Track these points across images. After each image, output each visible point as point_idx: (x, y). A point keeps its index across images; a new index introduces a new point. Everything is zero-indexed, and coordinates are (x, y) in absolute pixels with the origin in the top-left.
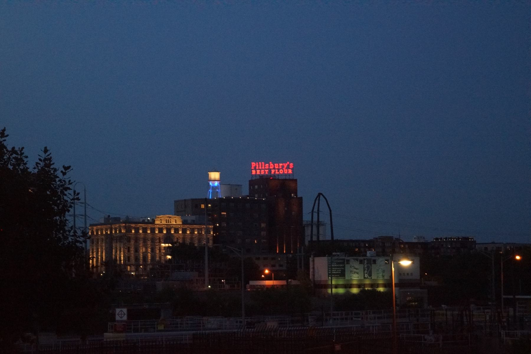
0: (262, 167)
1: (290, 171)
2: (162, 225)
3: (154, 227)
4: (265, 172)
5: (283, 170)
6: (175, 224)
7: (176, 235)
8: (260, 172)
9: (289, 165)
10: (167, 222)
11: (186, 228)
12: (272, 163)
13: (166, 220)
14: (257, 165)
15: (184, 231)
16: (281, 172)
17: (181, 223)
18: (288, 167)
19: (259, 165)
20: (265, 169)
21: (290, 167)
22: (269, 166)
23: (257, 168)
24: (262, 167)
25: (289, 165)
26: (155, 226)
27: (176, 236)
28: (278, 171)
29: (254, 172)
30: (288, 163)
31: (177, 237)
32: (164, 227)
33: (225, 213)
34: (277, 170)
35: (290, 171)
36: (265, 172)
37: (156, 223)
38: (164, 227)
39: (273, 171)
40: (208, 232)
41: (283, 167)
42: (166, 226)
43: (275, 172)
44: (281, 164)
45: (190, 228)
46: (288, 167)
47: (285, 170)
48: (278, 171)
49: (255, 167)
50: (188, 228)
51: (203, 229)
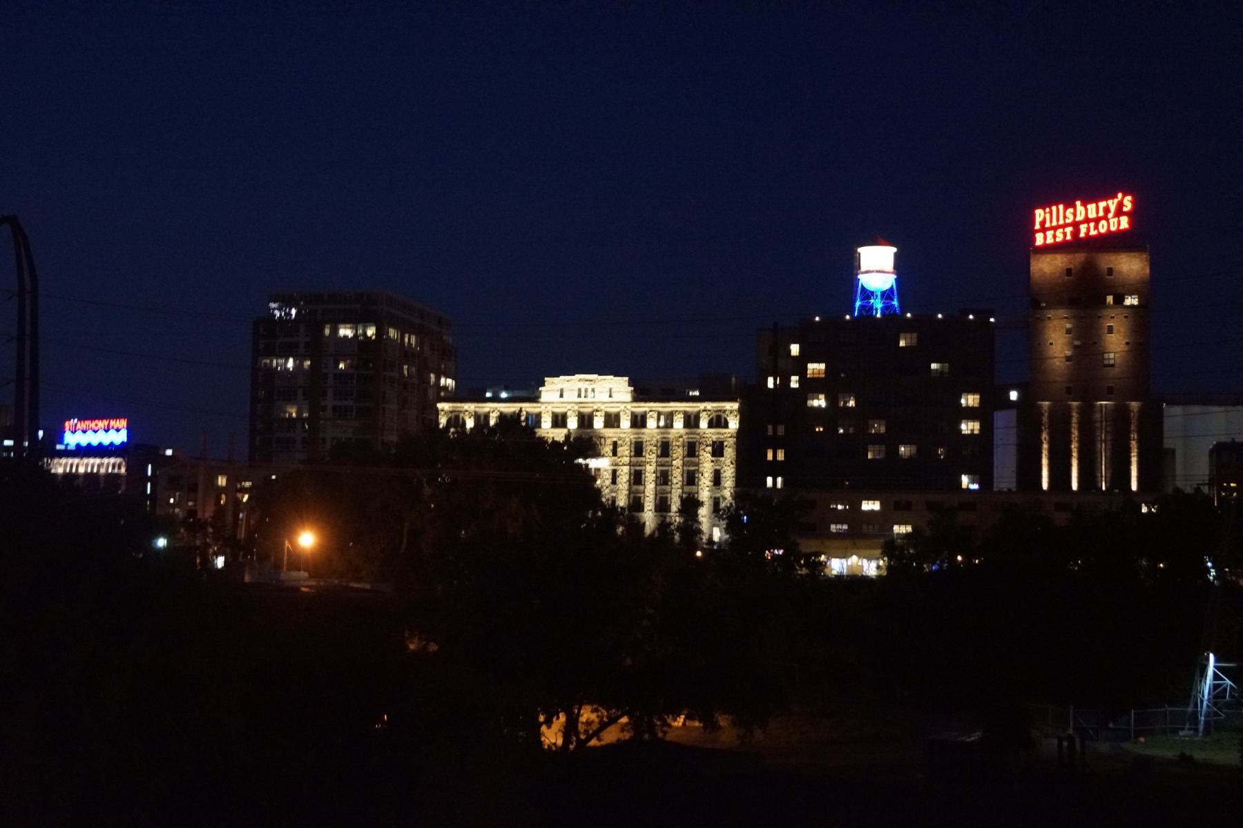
0: (1058, 220)
1: (1124, 223)
2: (564, 405)
3: (537, 410)
4: (1065, 234)
5: (1107, 220)
6: (610, 400)
7: (609, 432)
8: (1055, 237)
9: (1121, 205)
10: (583, 394)
11: (645, 412)
12: (1082, 205)
13: (580, 390)
14: (1048, 216)
15: (639, 421)
16: (1103, 229)
17: (629, 397)
18: (1119, 212)
19: (1051, 213)
20: (1065, 225)
21: (1125, 209)
22: (1075, 215)
23: (1048, 225)
24: (1058, 220)
25: (1121, 205)
26: (540, 407)
27: (610, 435)
28: (1096, 227)
29: (1039, 239)
30: (1120, 195)
31: (615, 439)
32: (570, 410)
33: (822, 366)
34: (1092, 225)
35: (1124, 223)
36: (1065, 234)
37: (543, 399)
38: (570, 410)
39: (1083, 228)
40: (718, 422)
41: (1107, 210)
42: (576, 407)
43: (1088, 229)
44: (1102, 204)
45: (659, 414)
46: (1119, 212)
47: (1111, 221)
48: (1096, 227)
49: (1043, 223)
50: (651, 411)
51: (703, 415)
